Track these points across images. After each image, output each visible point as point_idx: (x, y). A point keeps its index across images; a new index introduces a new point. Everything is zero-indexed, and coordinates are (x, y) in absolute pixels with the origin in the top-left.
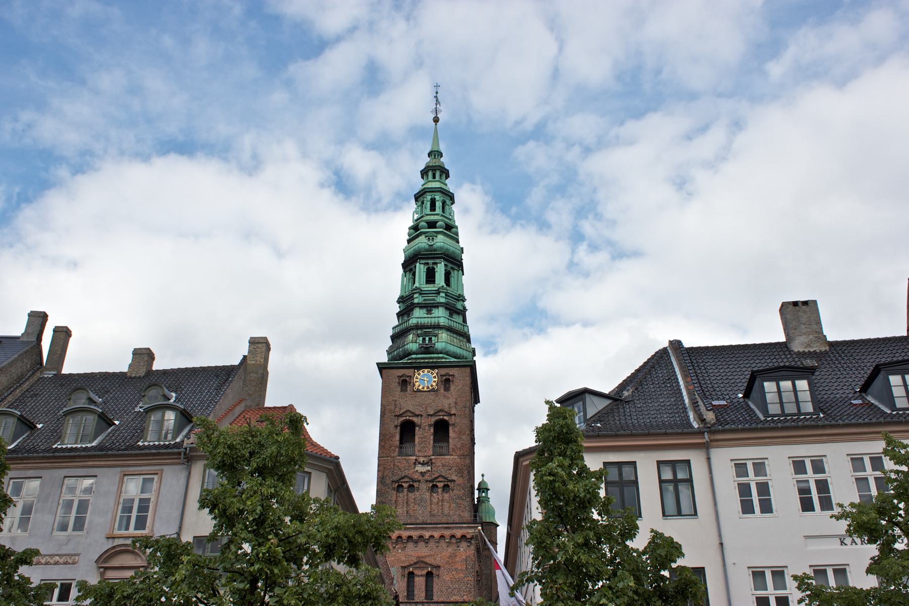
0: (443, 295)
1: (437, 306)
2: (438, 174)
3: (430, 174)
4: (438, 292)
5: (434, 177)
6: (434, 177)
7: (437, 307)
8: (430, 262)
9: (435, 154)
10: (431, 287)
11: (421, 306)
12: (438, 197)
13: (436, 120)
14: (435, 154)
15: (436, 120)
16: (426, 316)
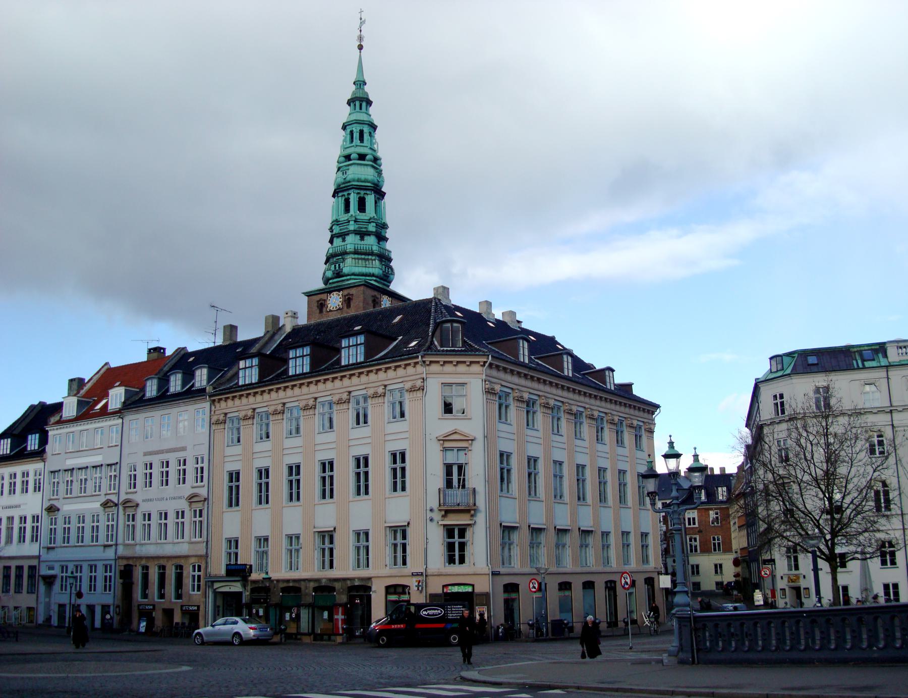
0: (374, 224)
1: (369, 234)
2: (364, 104)
3: (358, 103)
4: (369, 221)
5: (361, 108)
6: (361, 108)
7: (369, 235)
8: (362, 192)
9: (360, 83)
10: (361, 216)
11: (356, 232)
12: (366, 129)
13: (360, 47)
14: (360, 83)
15: (360, 47)
16: (359, 242)
